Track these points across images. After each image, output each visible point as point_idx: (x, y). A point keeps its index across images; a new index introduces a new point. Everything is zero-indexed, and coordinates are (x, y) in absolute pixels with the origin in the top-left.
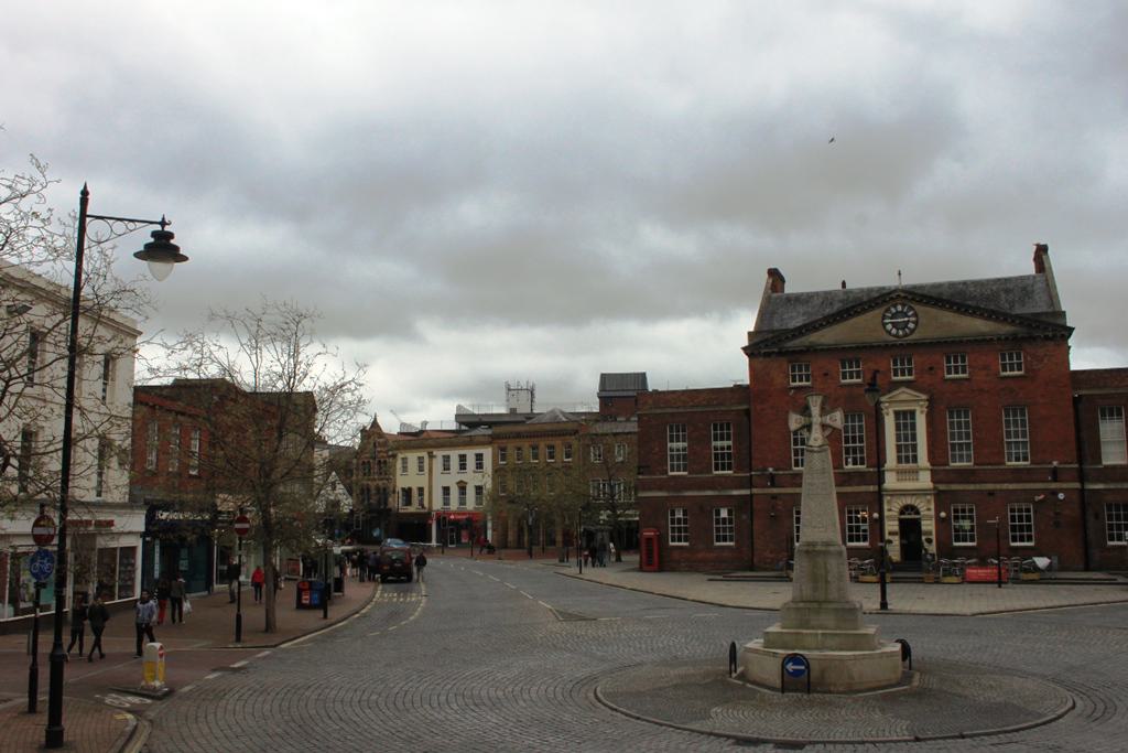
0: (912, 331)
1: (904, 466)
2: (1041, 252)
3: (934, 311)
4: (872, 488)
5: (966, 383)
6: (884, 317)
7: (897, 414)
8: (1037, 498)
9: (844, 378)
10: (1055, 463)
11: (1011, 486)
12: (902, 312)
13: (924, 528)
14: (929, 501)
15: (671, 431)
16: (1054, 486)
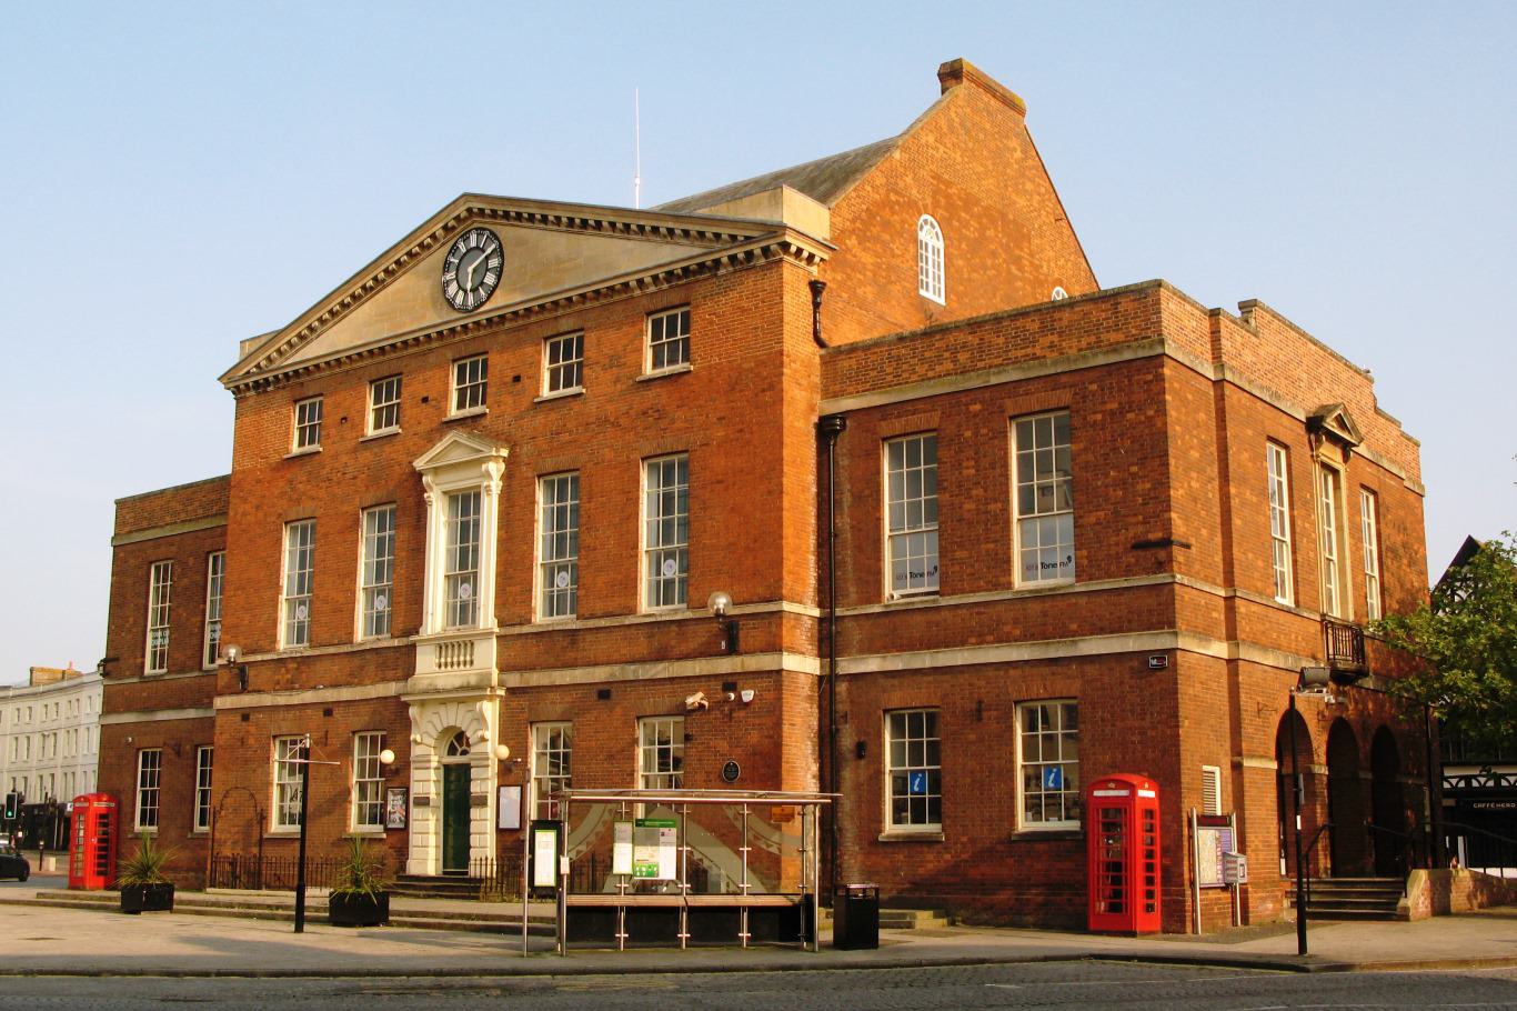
13: (475, 788)
16: (725, 665)
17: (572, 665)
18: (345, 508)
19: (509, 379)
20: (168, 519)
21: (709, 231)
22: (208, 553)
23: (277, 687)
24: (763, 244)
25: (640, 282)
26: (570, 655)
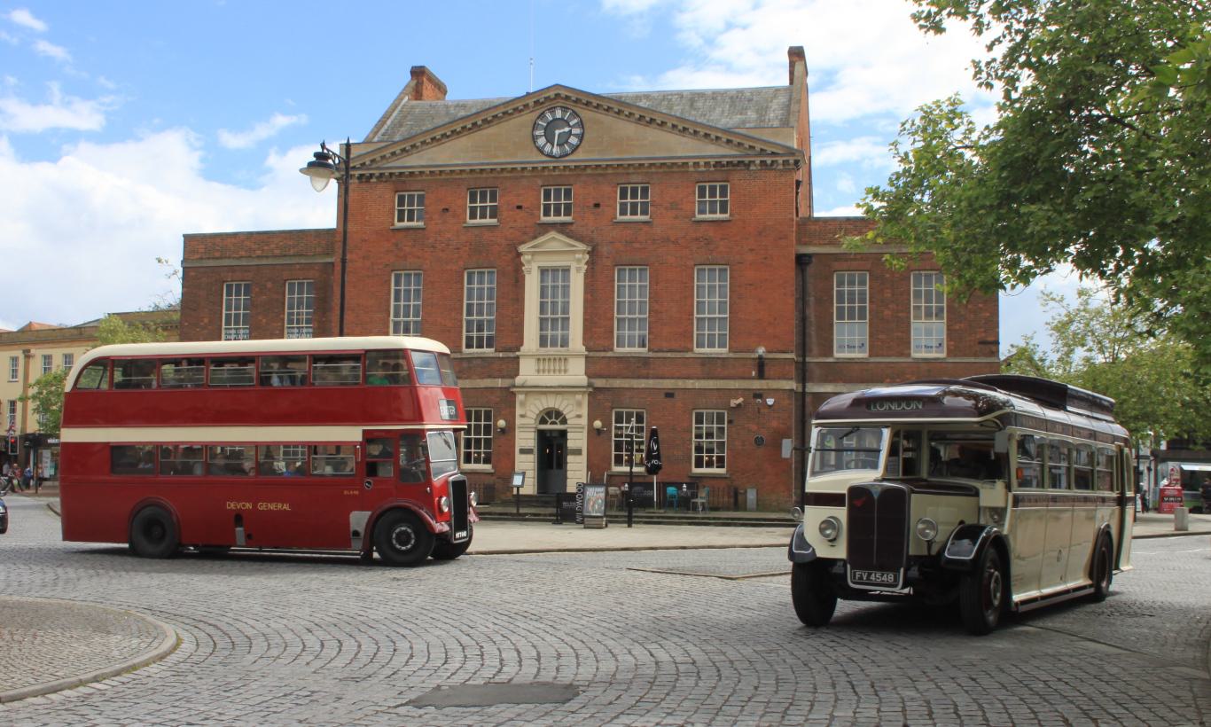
0: (575, 149)
1: (550, 350)
2: (797, 54)
3: (608, 119)
4: (499, 383)
5: (646, 228)
6: (535, 126)
7: (543, 271)
8: (734, 403)
9: (473, 216)
10: (761, 351)
11: (698, 384)
12: (562, 119)
13: (571, 444)
14: (579, 404)
15: (229, 294)
16: (757, 385)
17: (647, 377)
18: (449, 268)
19: (591, 205)
20: (243, 253)
21: (747, 144)
22: (285, 281)
24: (785, 159)
25: (696, 165)
26: (644, 372)
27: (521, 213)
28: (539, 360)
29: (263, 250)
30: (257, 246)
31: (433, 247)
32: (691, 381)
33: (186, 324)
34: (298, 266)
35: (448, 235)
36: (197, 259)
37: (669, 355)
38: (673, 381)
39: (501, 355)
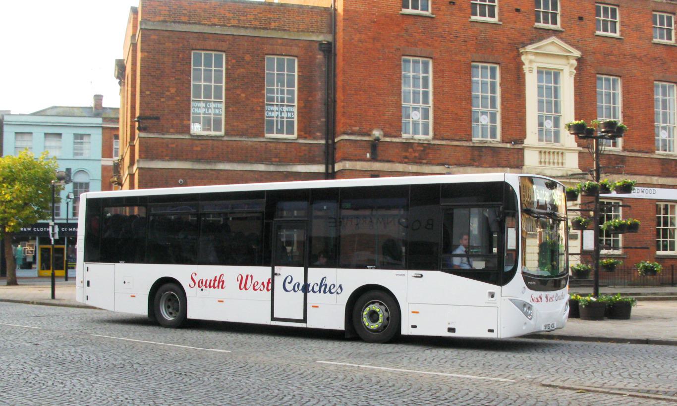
1: (543, 144)
7: (540, 72)
18: (457, 58)
19: (576, 17)
20: (216, 21)
23: (406, 160)
27: (520, 16)
28: (540, 152)
29: (239, 20)
30: (231, 15)
31: (442, 37)
32: (656, 178)
33: (148, 93)
34: (280, 41)
35: (456, 27)
36: (159, 21)
37: (640, 155)
38: (643, 177)
39: (508, 146)
